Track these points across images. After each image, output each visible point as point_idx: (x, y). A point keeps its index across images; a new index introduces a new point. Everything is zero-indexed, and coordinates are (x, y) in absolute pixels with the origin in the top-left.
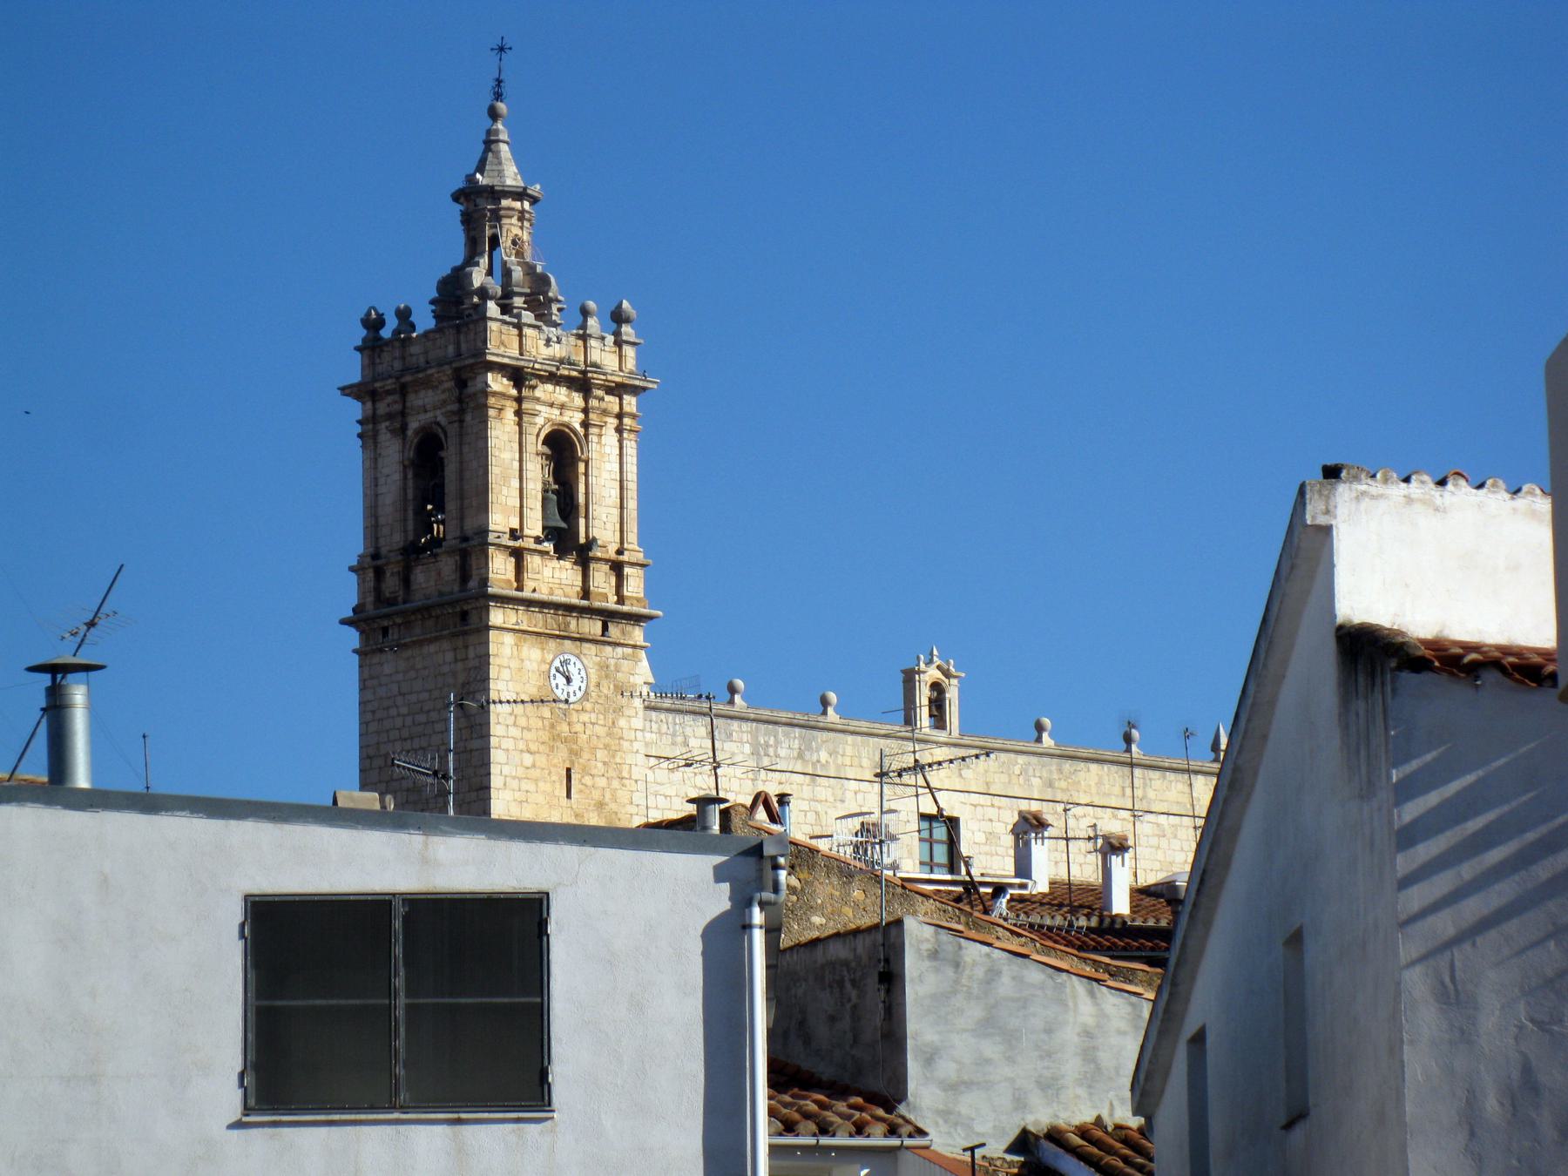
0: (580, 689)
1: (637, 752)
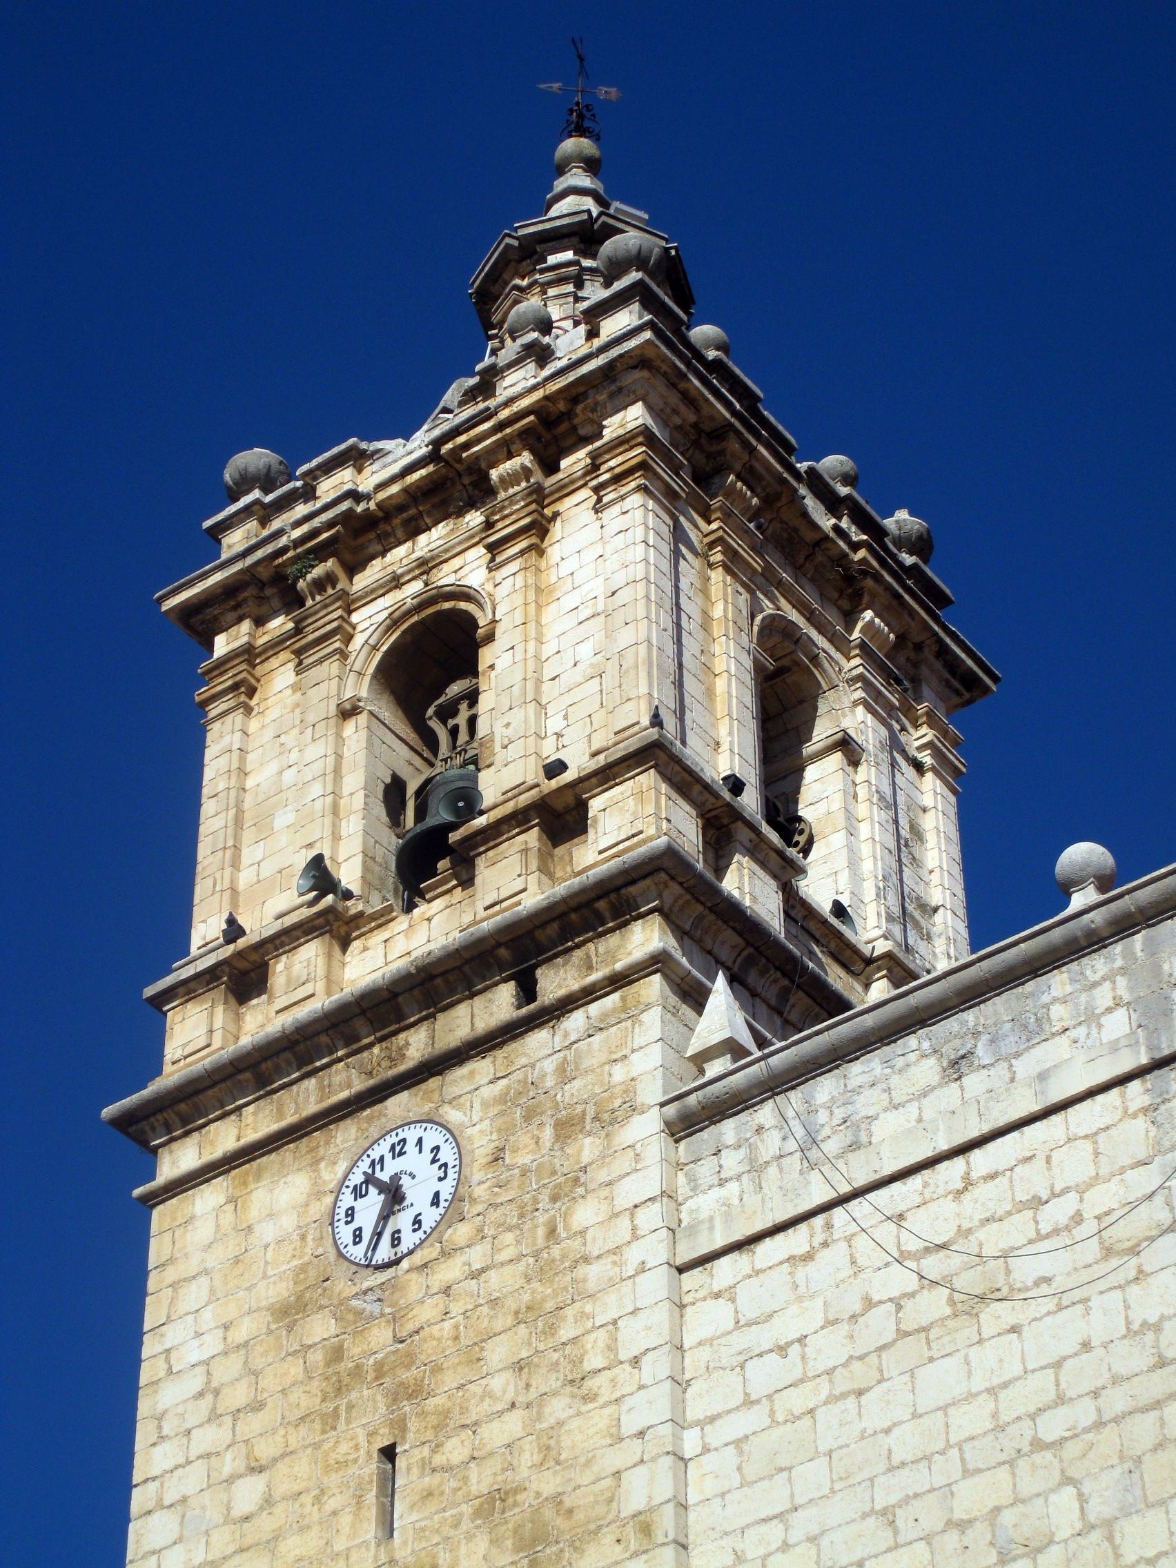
0: (435, 1202)
1: (642, 1268)
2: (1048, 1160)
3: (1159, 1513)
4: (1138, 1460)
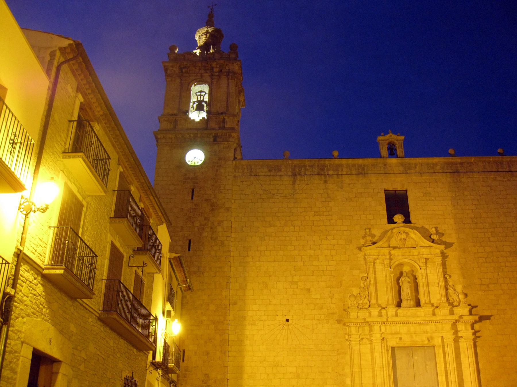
4: (287, 221)
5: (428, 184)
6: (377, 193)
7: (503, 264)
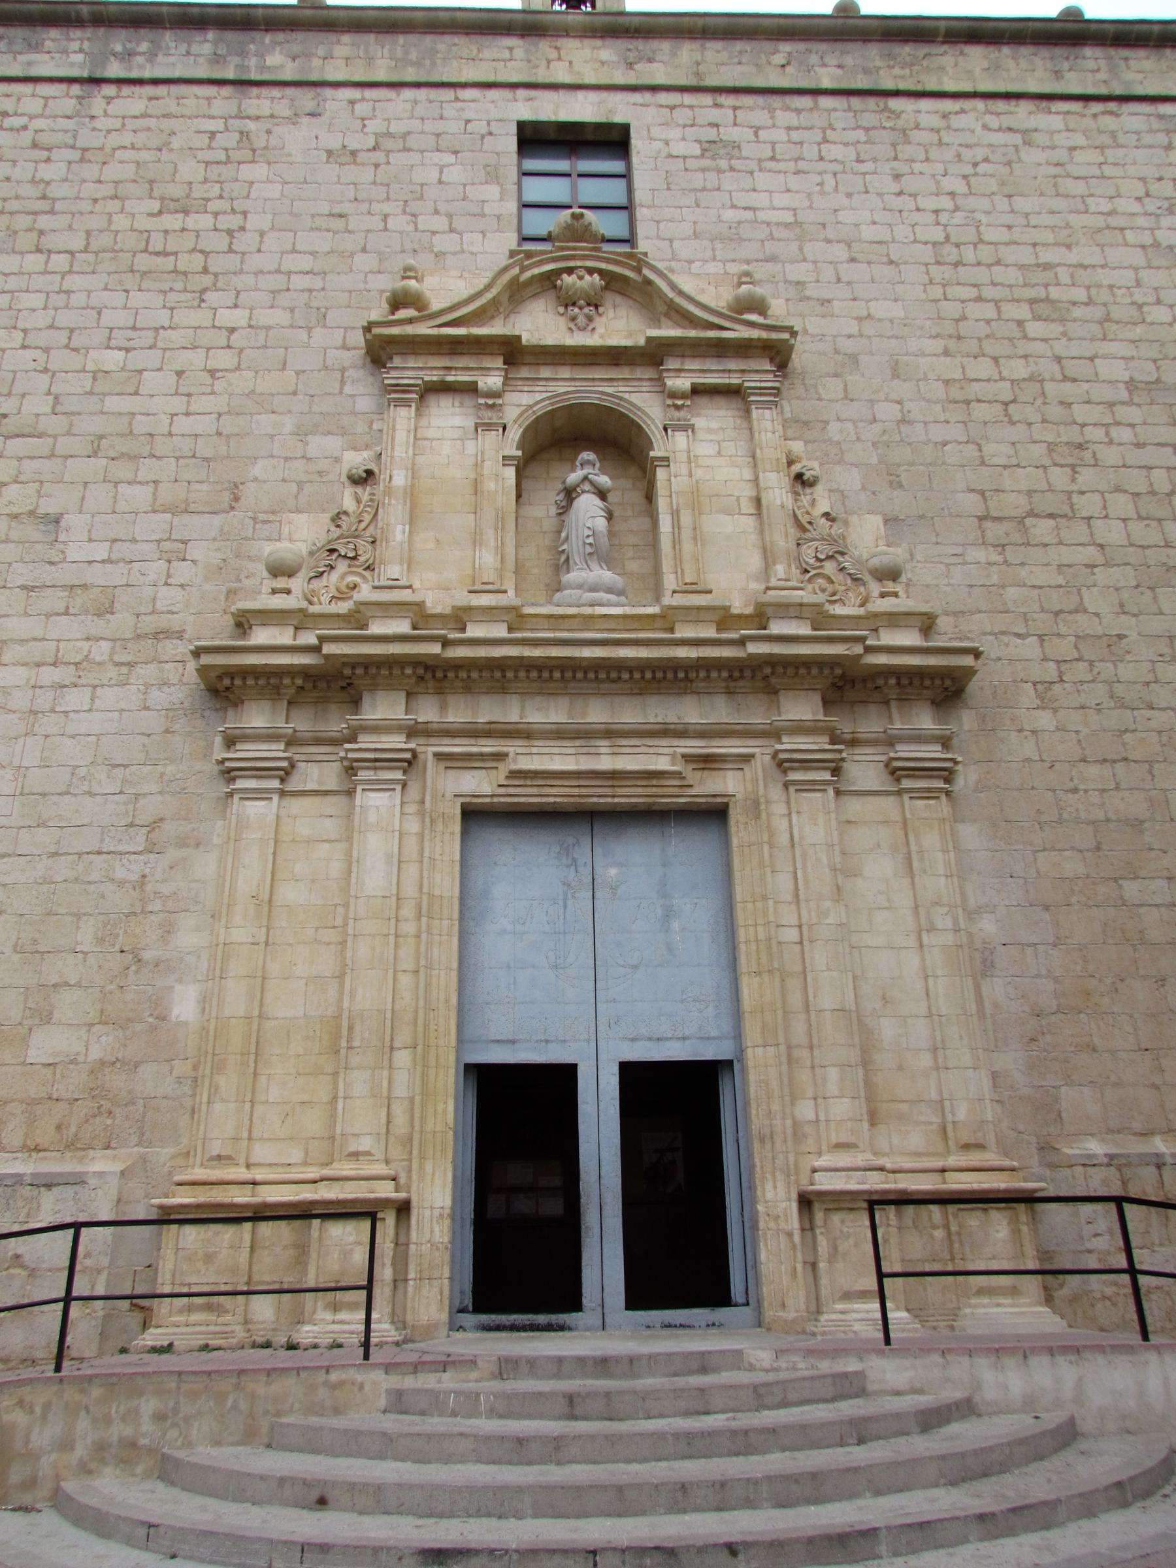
2: (19, 100)
3: (18, 257)
4: (16, 232)
5: (730, 112)
6: (483, 137)
7: (1098, 434)
